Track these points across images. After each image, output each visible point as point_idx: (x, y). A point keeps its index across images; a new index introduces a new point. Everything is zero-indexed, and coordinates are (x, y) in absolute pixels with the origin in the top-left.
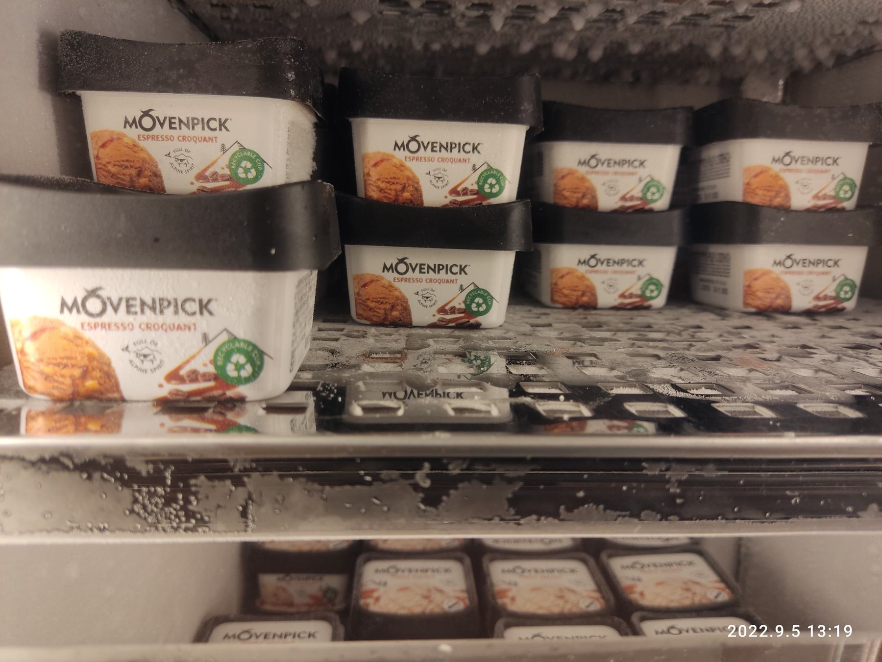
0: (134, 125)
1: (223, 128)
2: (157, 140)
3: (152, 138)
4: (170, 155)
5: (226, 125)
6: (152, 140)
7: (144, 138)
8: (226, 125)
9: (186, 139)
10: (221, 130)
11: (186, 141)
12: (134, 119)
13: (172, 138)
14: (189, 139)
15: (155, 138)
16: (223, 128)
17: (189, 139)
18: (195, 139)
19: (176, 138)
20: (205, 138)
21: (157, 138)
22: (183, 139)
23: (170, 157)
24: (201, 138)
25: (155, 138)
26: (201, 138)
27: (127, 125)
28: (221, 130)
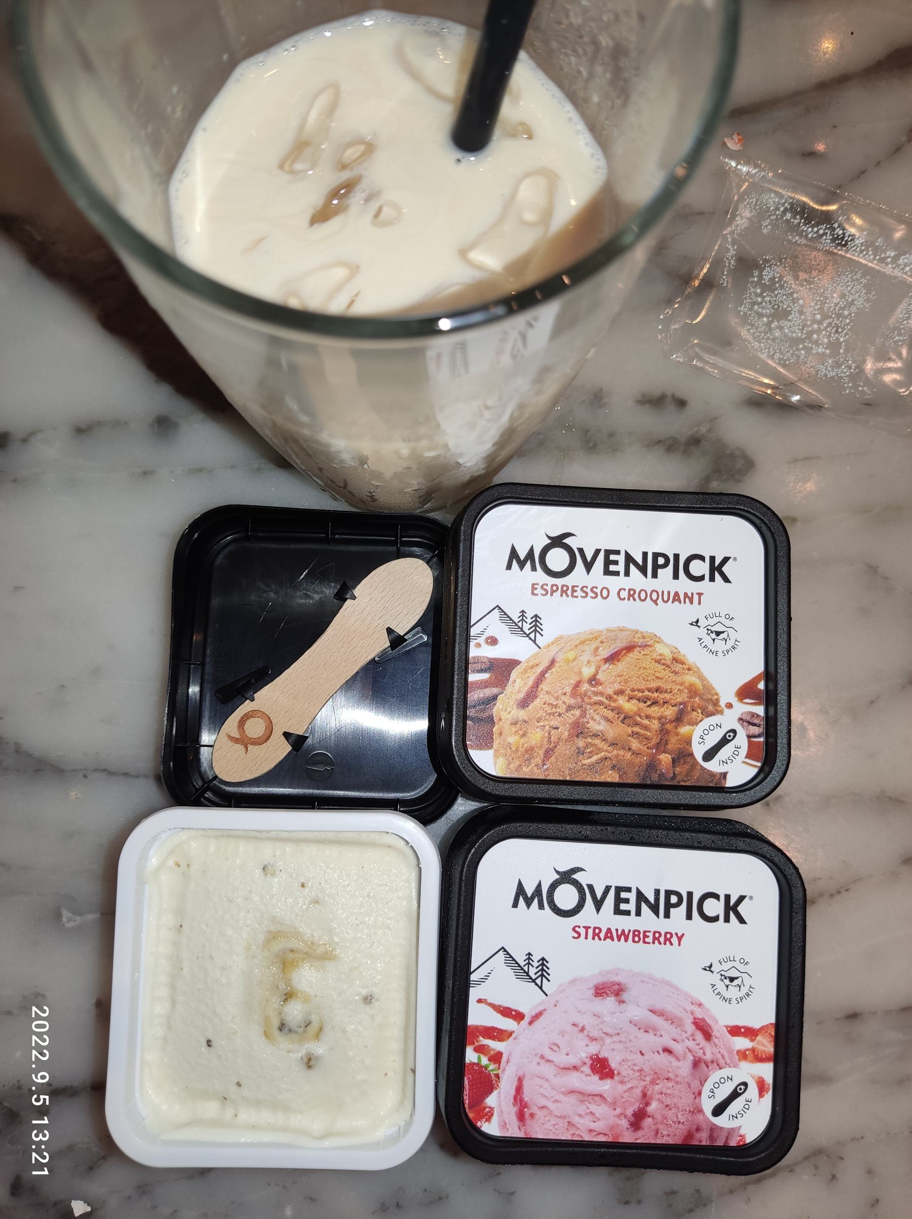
0: (528, 564)
1: (717, 575)
2: (573, 596)
3: (563, 591)
4: (712, 969)
5: (725, 569)
6: (562, 595)
7: (546, 590)
8: (725, 569)
9: (636, 596)
10: (712, 579)
11: (635, 600)
12: (531, 551)
13: (605, 593)
14: (643, 595)
15: (569, 592)
16: (717, 575)
17: (643, 595)
18: (654, 596)
19: (614, 593)
20: (677, 594)
21: (573, 591)
22: (630, 596)
23: (712, 972)
24: (669, 592)
25: (569, 592)
26: (669, 592)
27: (515, 564)
28: (712, 579)
